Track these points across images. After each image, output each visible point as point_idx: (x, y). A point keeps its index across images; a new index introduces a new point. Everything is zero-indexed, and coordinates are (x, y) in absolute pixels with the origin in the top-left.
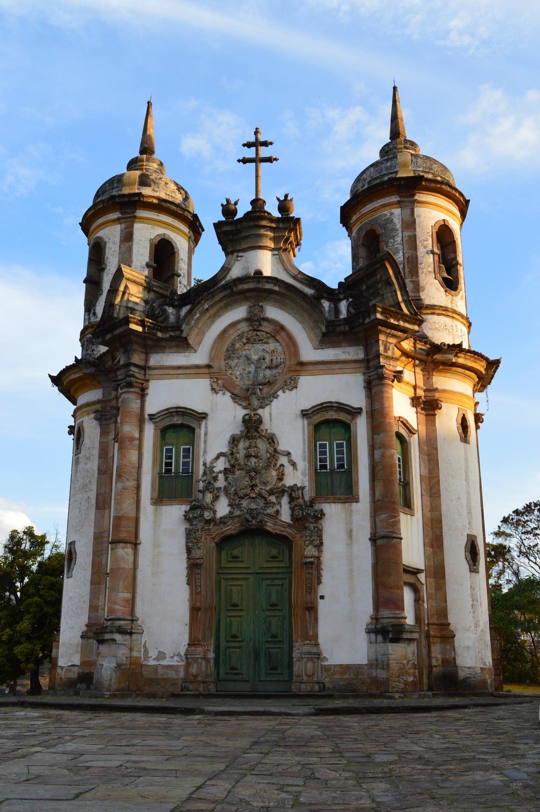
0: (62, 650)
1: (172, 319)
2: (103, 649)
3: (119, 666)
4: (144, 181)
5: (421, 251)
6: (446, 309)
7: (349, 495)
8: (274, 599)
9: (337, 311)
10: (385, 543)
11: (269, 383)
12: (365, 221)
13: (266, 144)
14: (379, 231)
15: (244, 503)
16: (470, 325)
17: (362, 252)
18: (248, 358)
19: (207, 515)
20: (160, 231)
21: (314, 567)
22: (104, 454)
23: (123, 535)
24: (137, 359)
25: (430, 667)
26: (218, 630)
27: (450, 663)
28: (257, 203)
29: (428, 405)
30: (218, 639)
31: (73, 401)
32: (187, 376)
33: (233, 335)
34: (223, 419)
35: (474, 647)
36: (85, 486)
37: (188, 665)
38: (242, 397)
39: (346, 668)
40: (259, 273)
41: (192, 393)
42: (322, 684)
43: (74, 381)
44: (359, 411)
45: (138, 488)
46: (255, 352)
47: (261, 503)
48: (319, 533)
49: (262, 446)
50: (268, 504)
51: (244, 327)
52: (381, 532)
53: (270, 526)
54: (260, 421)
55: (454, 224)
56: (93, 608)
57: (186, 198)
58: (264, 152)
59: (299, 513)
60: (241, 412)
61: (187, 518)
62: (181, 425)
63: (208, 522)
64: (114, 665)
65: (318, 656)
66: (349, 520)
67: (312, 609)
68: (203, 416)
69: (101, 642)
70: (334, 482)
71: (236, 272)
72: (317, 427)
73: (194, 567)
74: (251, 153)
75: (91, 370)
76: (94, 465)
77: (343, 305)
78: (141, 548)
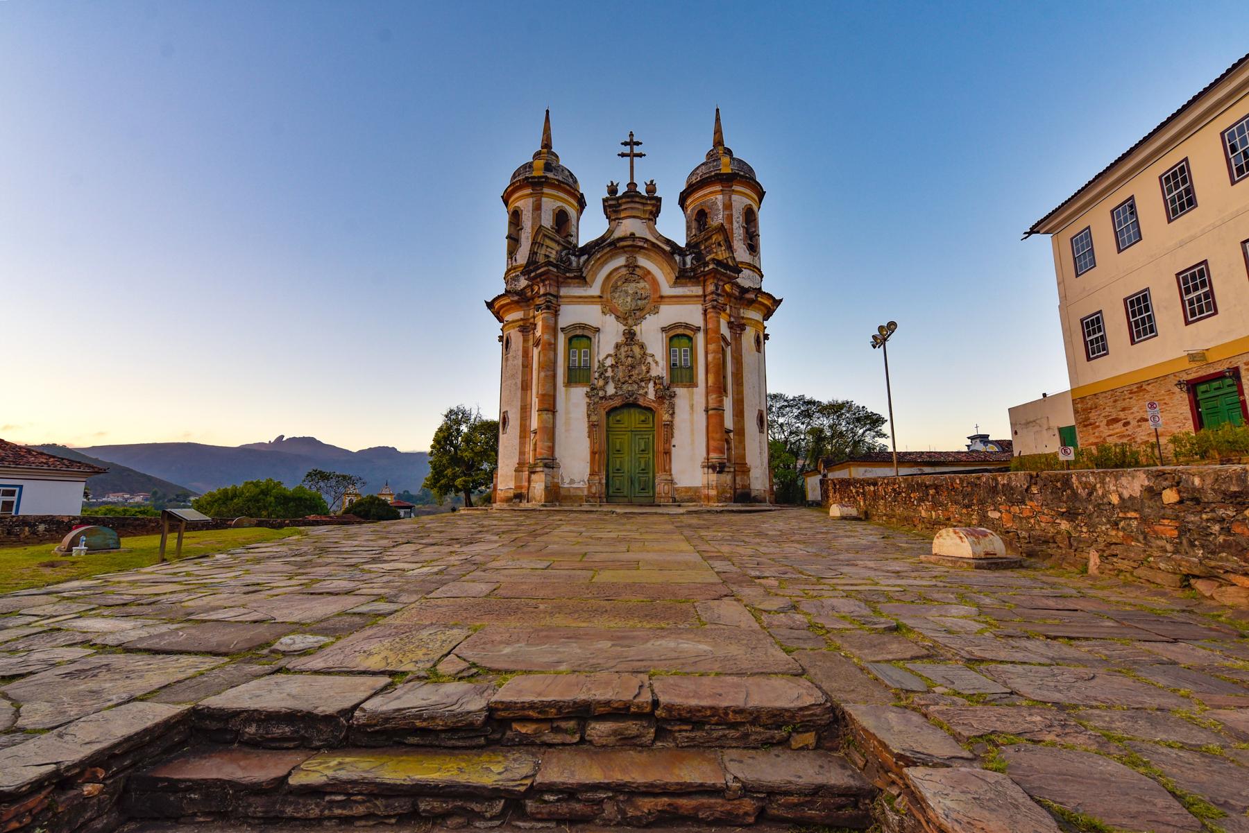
0: (499, 480)
1: (574, 264)
2: (533, 476)
3: (546, 487)
5: (735, 225)
6: (749, 265)
7: (692, 383)
8: (643, 447)
9: (685, 263)
11: (640, 309)
12: (697, 203)
13: (638, 144)
14: (707, 211)
15: (625, 387)
16: (762, 276)
17: (694, 224)
18: (626, 292)
19: (601, 394)
20: (559, 204)
21: (670, 426)
22: (526, 354)
23: (546, 406)
24: (553, 290)
25: (735, 489)
26: (608, 466)
27: (747, 487)
28: (632, 185)
29: (738, 327)
30: (607, 471)
31: (501, 320)
32: (585, 303)
33: (616, 276)
34: (610, 333)
35: (759, 479)
36: (513, 376)
37: (590, 487)
39: (688, 489)
40: (633, 234)
41: (590, 314)
42: (674, 501)
43: (503, 306)
44: (698, 329)
45: (554, 376)
46: (631, 288)
47: (636, 386)
48: (672, 406)
49: (636, 350)
50: (640, 387)
51: (624, 271)
52: (711, 406)
53: (641, 402)
54: (635, 334)
55: (755, 208)
56: (522, 453)
57: (575, 181)
58: (637, 150)
59: (660, 394)
60: (622, 328)
61: (588, 395)
62: (582, 336)
63: (601, 398)
64: (542, 486)
65: (672, 481)
66: (691, 399)
67: (668, 453)
68: (598, 330)
69: (534, 472)
71: (617, 235)
72: (671, 339)
73: (592, 426)
74: (627, 150)
75: (516, 298)
76: (519, 361)
77: (688, 259)
78: (557, 414)
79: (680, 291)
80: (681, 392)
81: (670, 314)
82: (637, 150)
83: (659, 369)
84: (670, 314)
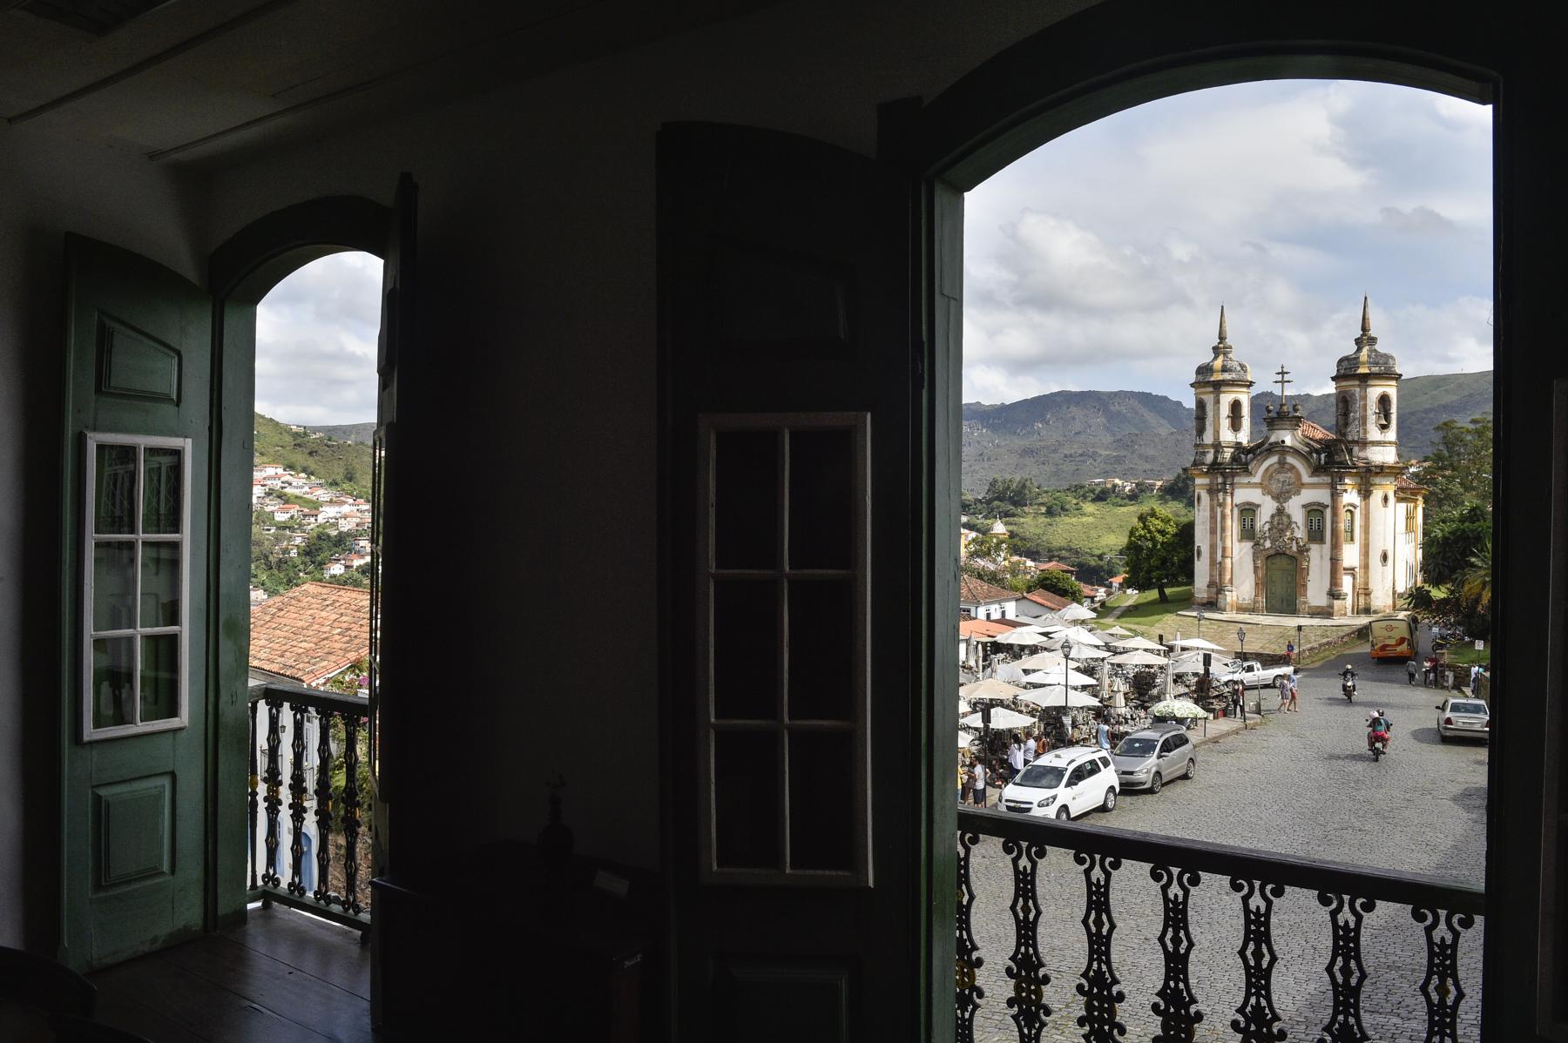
4: (1224, 369)
5: (1369, 412)
7: (1322, 540)
10: (1335, 561)
22: (1212, 510)
29: (1366, 494)
34: (1268, 507)
38: (1276, 498)
46: (1281, 477)
58: (1286, 377)
60: (1276, 505)
62: (1248, 510)
70: (1316, 535)
71: (1272, 440)
73: (1256, 568)
74: (1279, 378)
76: (1208, 514)
79: (1315, 480)
80: (1314, 548)
81: (1307, 496)
82: (1286, 377)
83: (1301, 533)
84: (1307, 496)
